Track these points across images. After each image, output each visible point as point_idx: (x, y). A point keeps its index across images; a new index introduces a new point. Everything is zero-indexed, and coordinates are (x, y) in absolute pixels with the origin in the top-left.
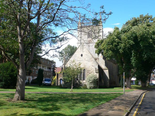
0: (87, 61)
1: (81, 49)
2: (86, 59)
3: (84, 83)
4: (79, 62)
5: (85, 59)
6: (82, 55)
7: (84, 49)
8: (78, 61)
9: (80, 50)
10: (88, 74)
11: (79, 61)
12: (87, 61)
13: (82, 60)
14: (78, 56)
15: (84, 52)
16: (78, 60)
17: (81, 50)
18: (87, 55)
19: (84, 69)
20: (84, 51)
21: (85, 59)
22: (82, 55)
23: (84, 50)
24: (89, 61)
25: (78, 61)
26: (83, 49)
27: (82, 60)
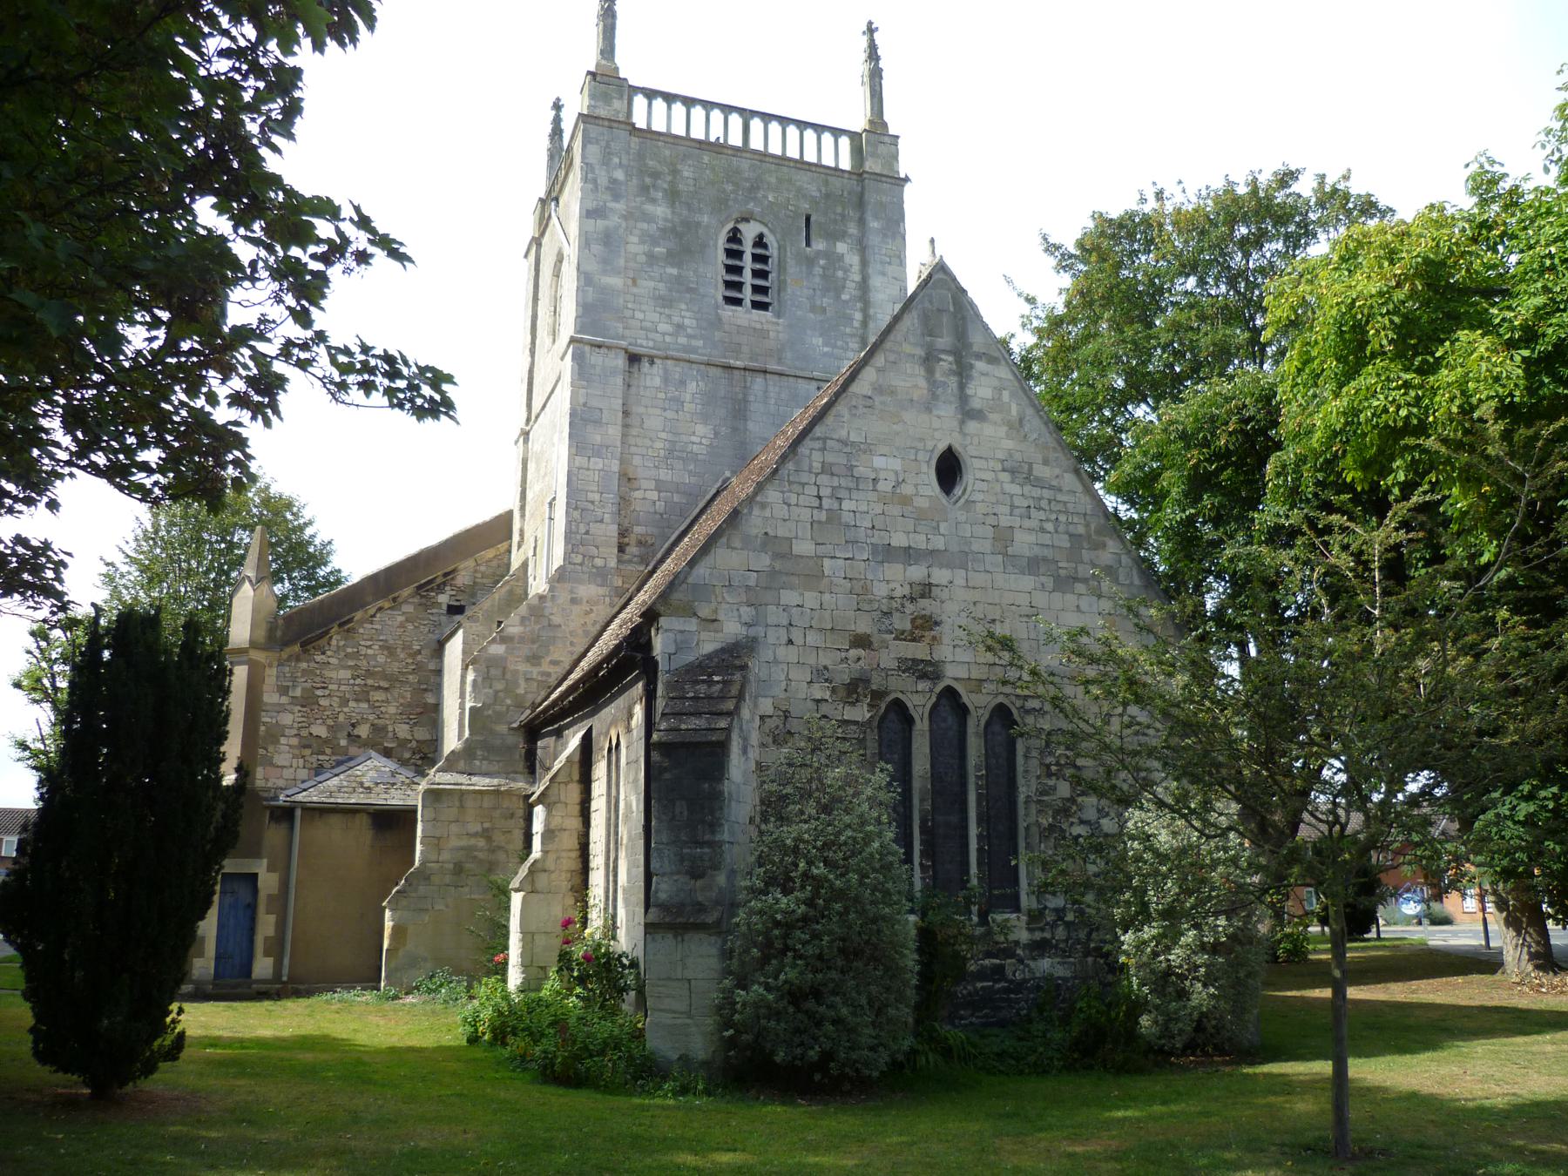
0: (1033, 565)
1: (929, 360)
2: (1024, 543)
3: (1008, 953)
4: (917, 573)
5: (1003, 537)
6: (949, 469)
7: (980, 365)
8: (887, 553)
9: (920, 371)
10: (1064, 789)
11: (908, 555)
12: (1033, 565)
13: (962, 559)
14: (884, 464)
15: (988, 430)
16: (899, 540)
17: (932, 382)
18: (1029, 479)
19: (1002, 714)
20: (976, 404)
21: (1003, 537)
22: (949, 469)
23: (981, 391)
24: (1064, 583)
25: (887, 553)
26: (962, 372)
27: (962, 559)
